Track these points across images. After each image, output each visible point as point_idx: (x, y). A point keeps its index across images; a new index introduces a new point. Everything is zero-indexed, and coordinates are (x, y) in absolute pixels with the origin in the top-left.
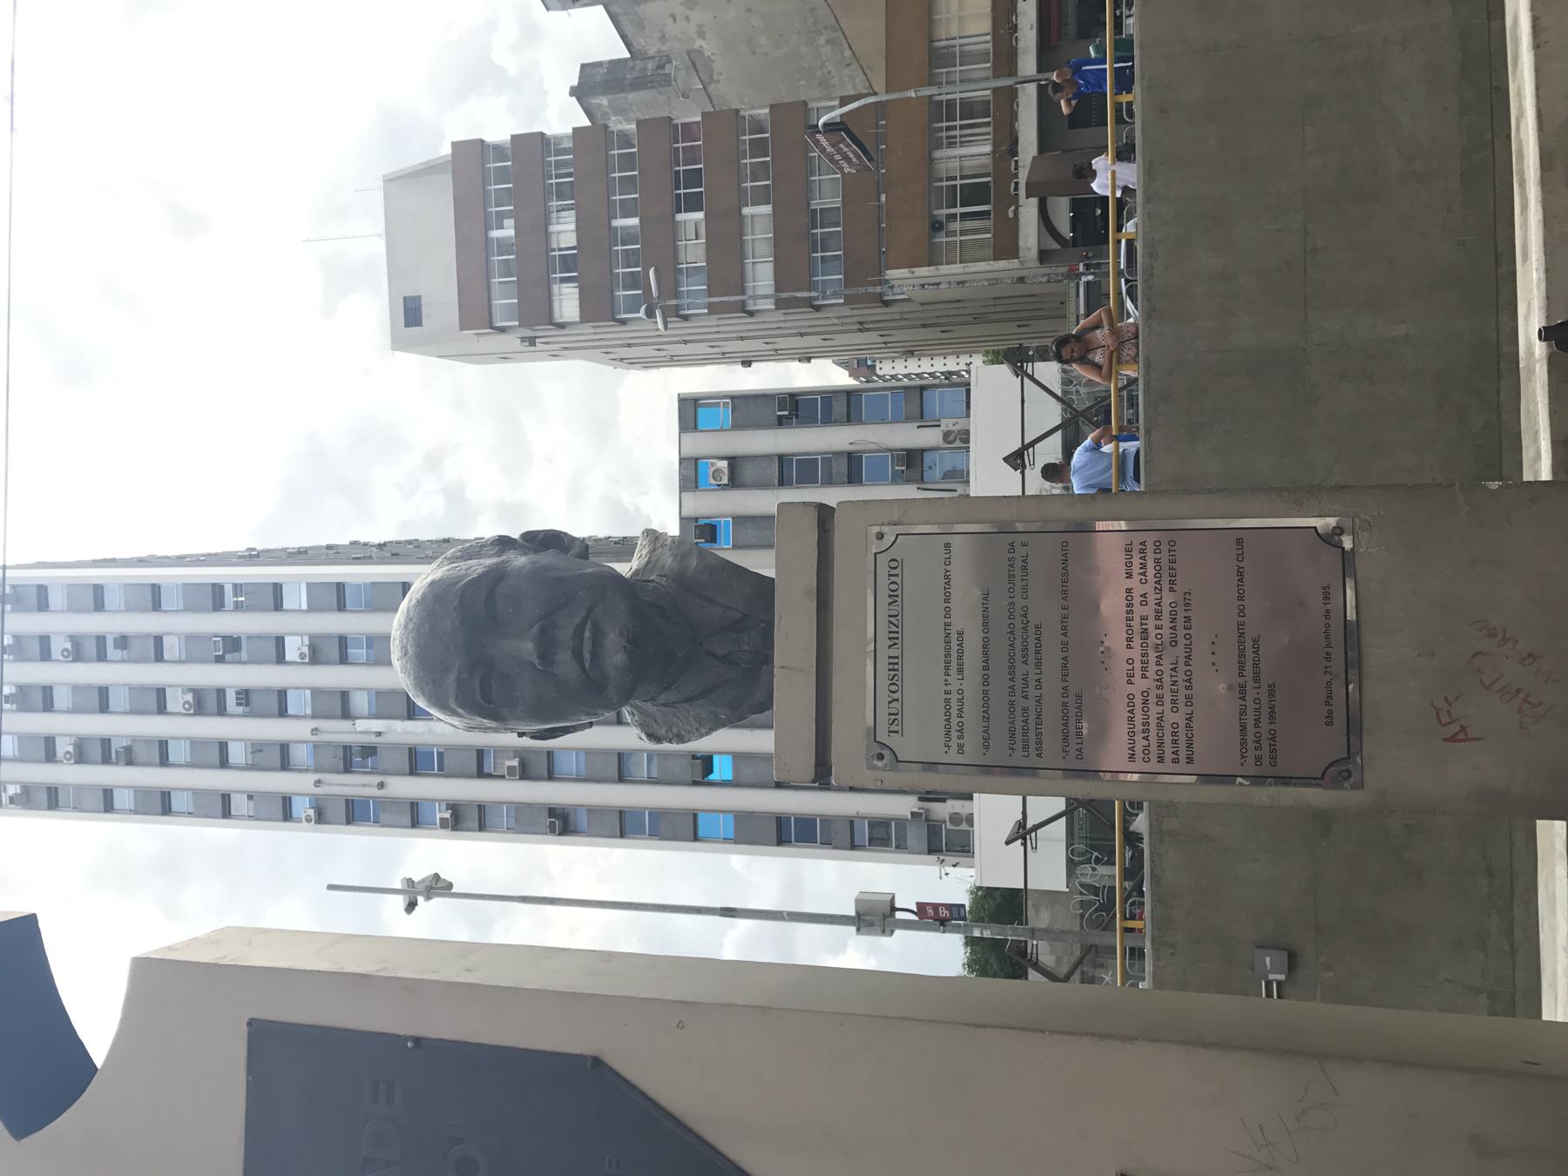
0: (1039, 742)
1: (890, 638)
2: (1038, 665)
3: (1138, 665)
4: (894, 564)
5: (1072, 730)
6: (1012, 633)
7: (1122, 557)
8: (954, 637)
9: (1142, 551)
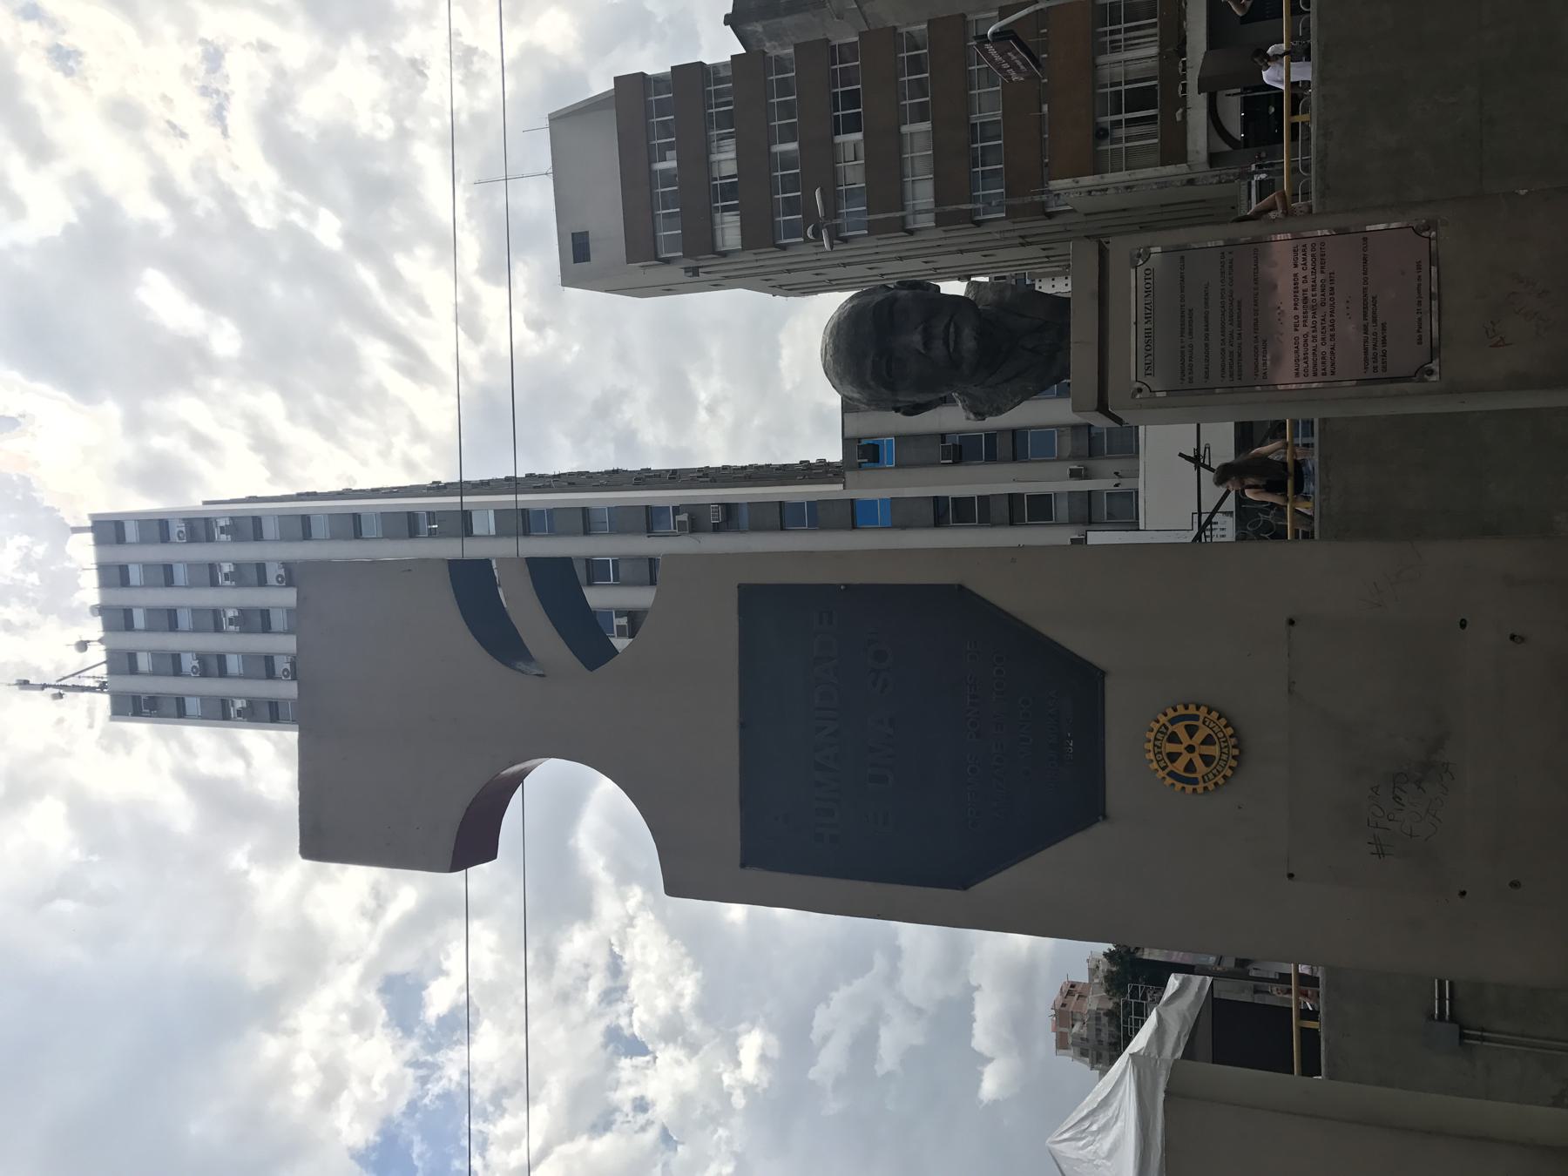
0: (1240, 370)
1: (1146, 318)
2: (1239, 325)
3: (1301, 319)
4: (1148, 272)
5: (1261, 362)
6: (1223, 307)
7: (1291, 255)
8: (1187, 312)
9: (1304, 250)
